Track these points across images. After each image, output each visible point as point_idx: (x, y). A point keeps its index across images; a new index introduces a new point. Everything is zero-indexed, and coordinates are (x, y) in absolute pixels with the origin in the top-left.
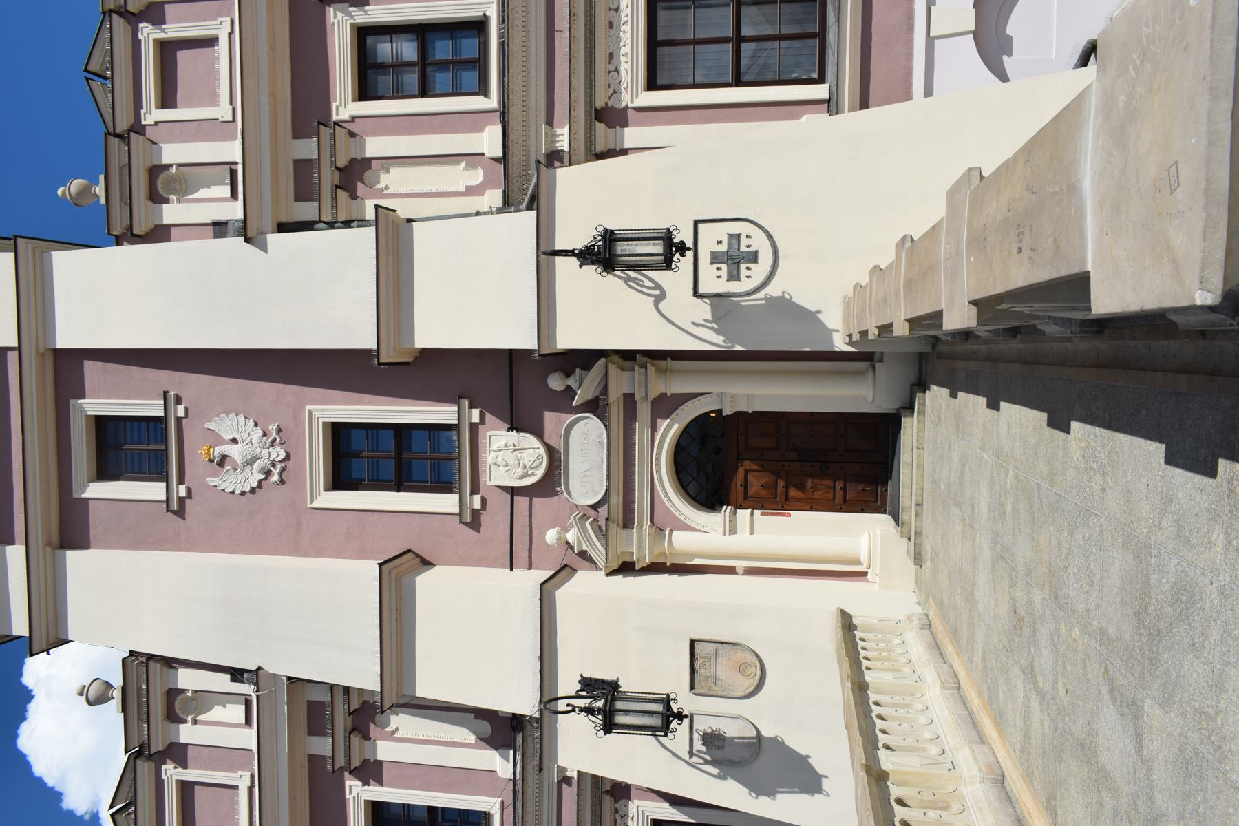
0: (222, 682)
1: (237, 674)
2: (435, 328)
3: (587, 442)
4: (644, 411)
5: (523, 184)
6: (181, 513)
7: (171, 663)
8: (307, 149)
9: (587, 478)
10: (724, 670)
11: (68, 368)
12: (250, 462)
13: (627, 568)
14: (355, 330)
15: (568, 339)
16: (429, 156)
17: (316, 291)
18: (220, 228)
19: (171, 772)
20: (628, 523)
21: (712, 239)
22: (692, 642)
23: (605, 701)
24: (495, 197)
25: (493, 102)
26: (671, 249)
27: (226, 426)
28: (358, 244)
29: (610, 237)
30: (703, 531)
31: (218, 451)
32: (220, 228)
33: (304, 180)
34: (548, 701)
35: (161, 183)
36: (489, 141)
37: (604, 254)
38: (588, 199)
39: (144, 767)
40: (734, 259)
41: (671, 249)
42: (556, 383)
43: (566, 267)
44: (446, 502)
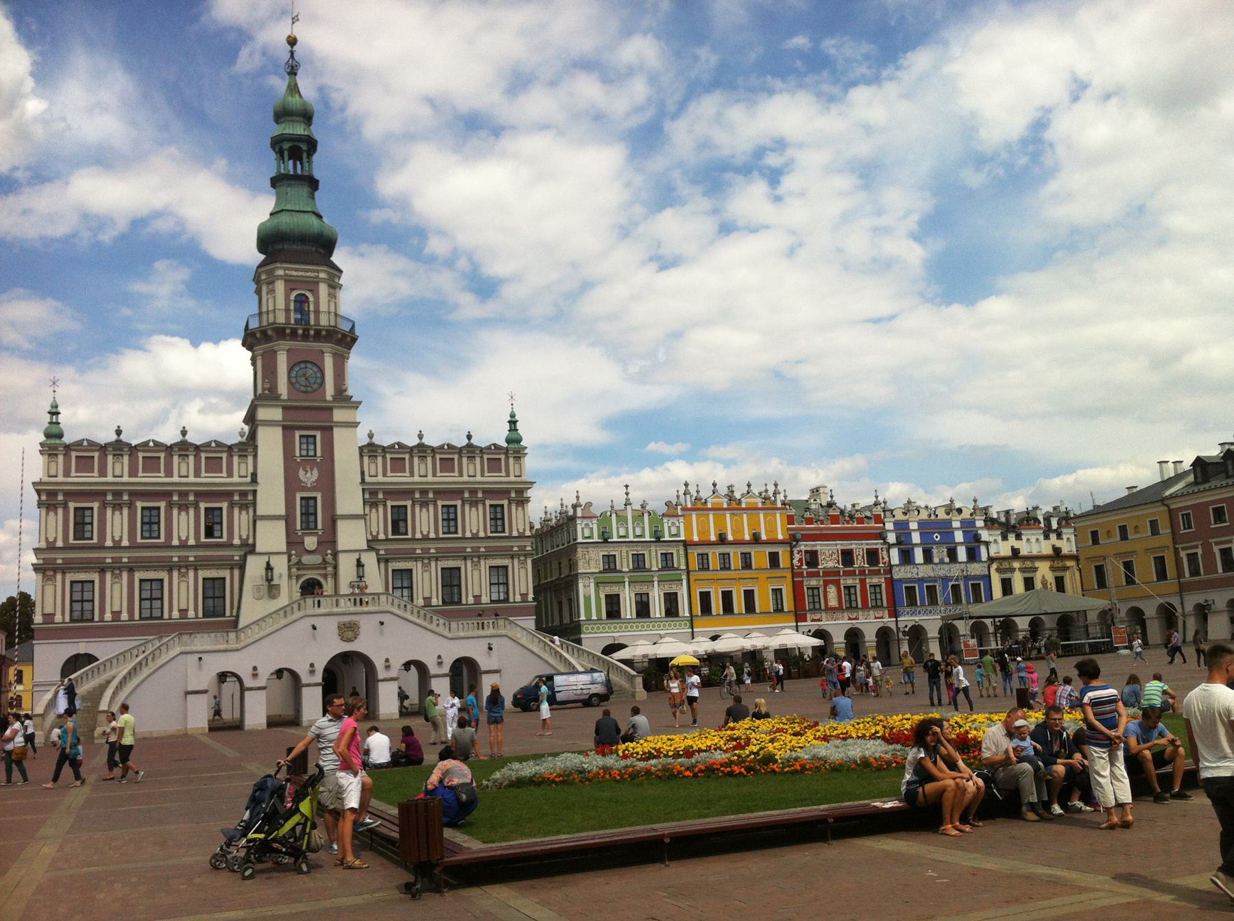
0: (251, 470)
1: (254, 475)
2: (341, 525)
3: (316, 559)
5: (372, 544)
7: (255, 456)
9: (306, 559)
10: (274, 591)
14: (341, 509)
15: (341, 557)
16: (379, 521)
17: (349, 498)
19: (224, 456)
23: (269, 568)
27: (316, 472)
28: (358, 508)
32: (363, 473)
33: (374, 493)
35: (373, 457)
36: (382, 536)
37: (359, 564)
38: (370, 560)
43: (356, 556)
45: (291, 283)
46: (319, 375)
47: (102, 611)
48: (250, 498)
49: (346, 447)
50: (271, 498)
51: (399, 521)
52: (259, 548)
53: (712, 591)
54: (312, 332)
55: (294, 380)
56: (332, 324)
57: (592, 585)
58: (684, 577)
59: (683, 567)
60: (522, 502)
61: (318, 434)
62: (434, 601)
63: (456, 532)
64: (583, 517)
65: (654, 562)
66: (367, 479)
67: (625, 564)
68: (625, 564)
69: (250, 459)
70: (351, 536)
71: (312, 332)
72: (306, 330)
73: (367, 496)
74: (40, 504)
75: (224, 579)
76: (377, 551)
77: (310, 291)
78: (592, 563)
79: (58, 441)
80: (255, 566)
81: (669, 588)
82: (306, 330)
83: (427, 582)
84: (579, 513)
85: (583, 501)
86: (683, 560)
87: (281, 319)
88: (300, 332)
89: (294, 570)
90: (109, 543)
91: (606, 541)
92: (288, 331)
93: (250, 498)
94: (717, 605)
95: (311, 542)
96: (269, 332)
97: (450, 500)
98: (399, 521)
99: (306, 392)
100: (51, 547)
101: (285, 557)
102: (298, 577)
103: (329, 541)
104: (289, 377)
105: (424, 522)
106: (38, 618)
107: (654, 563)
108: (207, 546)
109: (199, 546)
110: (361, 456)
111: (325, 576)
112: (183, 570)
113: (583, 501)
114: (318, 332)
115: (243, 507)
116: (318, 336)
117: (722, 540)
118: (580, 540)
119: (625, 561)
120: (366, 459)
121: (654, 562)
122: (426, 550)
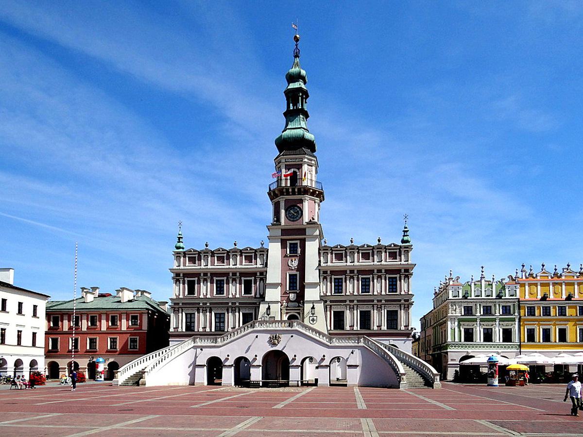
0: (265, 261)
1: (267, 263)
4: (298, 311)
5: (323, 299)
6: (286, 256)
8: (329, 272)
11: (303, 242)
12: (292, 264)
13: (281, 310)
17: (312, 275)
18: (320, 261)
20: (286, 310)
21: (315, 318)
22: (274, 317)
24: (322, 294)
26: (313, 314)
29: (314, 308)
30: (285, 318)
31: (293, 260)
32: (320, 261)
33: (325, 272)
34: (269, 303)
36: (329, 294)
37: (313, 308)
38: (320, 307)
39: (254, 251)
40: (313, 320)
41: (313, 314)
42: (302, 301)
44: (288, 289)
45: (288, 167)
46: (300, 212)
47: (199, 327)
49: (312, 248)
50: (274, 274)
51: (339, 287)
52: (267, 299)
53: (553, 329)
54: (296, 190)
55: (288, 216)
56: (309, 185)
57: (456, 323)
58: (517, 320)
59: (516, 314)
60: (407, 277)
61: (298, 242)
62: (355, 328)
63: (369, 292)
64: (453, 285)
65: (498, 312)
66: (322, 264)
67: (479, 312)
68: (479, 312)
69: (265, 255)
70: (311, 294)
71: (296, 190)
72: (293, 190)
73: (321, 273)
74: (173, 278)
75: (252, 313)
76: (325, 302)
77: (299, 169)
78: (458, 310)
79: (181, 250)
80: (263, 308)
81: (507, 325)
82: (293, 190)
83: (352, 319)
84: (451, 283)
85: (454, 277)
86: (516, 311)
87: (283, 185)
88: (290, 190)
89: (284, 311)
90: (202, 296)
91: (466, 298)
92: (284, 190)
93: (265, 274)
94: (539, 335)
95: (292, 296)
96: (276, 192)
97: (366, 277)
98: (339, 287)
99: (293, 221)
100: (178, 298)
101: (280, 304)
102: (287, 313)
103: (301, 297)
104: (286, 215)
105: (351, 288)
106: (172, 330)
107: (497, 311)
108: (243, 298)
109: (242, 298)
110: (319, 253)
111: (299, 313)
112: (234, 309)
113: (454, 277)
114: (299, 189)
115: (261, 279)
116: (300, 193)
117: (544, 298)
118: (451, 297)
119: (478, 310)
120: (322, 254)
121: (498, 312)
122: (353, 301)
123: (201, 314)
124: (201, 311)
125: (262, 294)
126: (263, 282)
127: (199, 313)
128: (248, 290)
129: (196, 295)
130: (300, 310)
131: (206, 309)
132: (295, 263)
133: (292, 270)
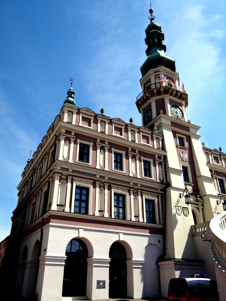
1: (163, 148)
7: (163, 140)
12: (183, 156)
25: (221, 194)
48: (162, 158)
49: (197, 145)
54: (179, 94)
88: (175, 93)
95: (190, 188)
111: (198, 209)
115: (160, 164)
123: (98, 189)
124: (98, 185)
125: (162, 179)
126: (162, 167)
127: (95, 187)
128: (148, 172)
129: (90, 164)
130: (198, 205)
131: (104, 185)
132: (186, 156)
133: (184, 161)
